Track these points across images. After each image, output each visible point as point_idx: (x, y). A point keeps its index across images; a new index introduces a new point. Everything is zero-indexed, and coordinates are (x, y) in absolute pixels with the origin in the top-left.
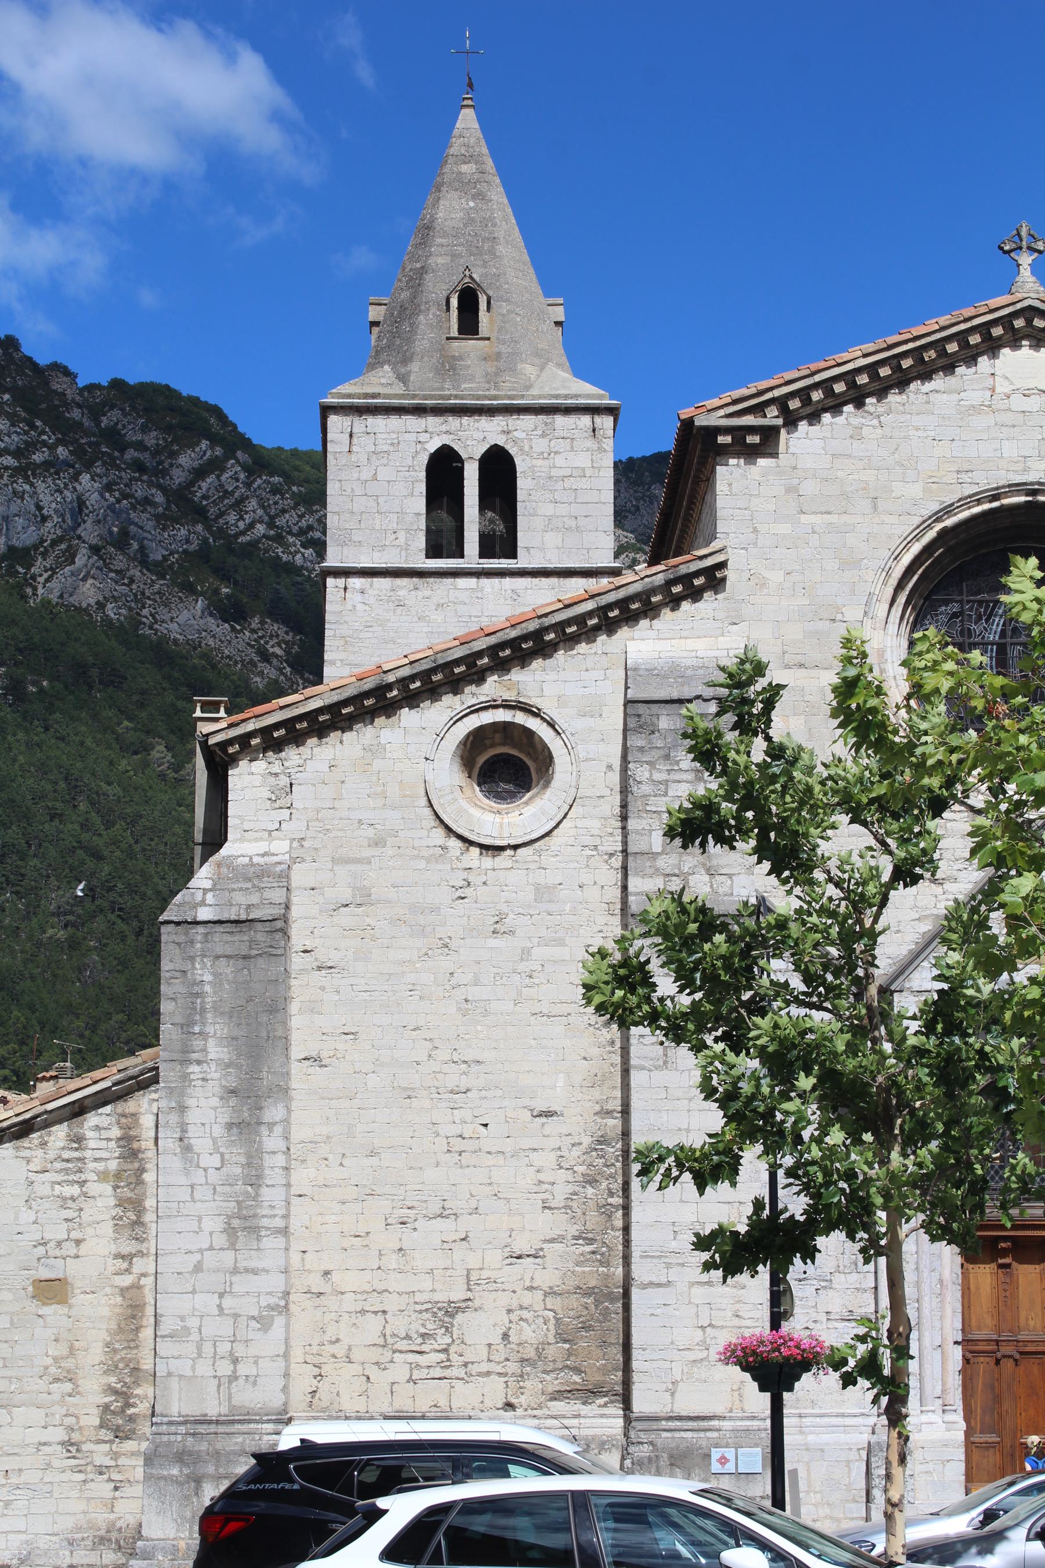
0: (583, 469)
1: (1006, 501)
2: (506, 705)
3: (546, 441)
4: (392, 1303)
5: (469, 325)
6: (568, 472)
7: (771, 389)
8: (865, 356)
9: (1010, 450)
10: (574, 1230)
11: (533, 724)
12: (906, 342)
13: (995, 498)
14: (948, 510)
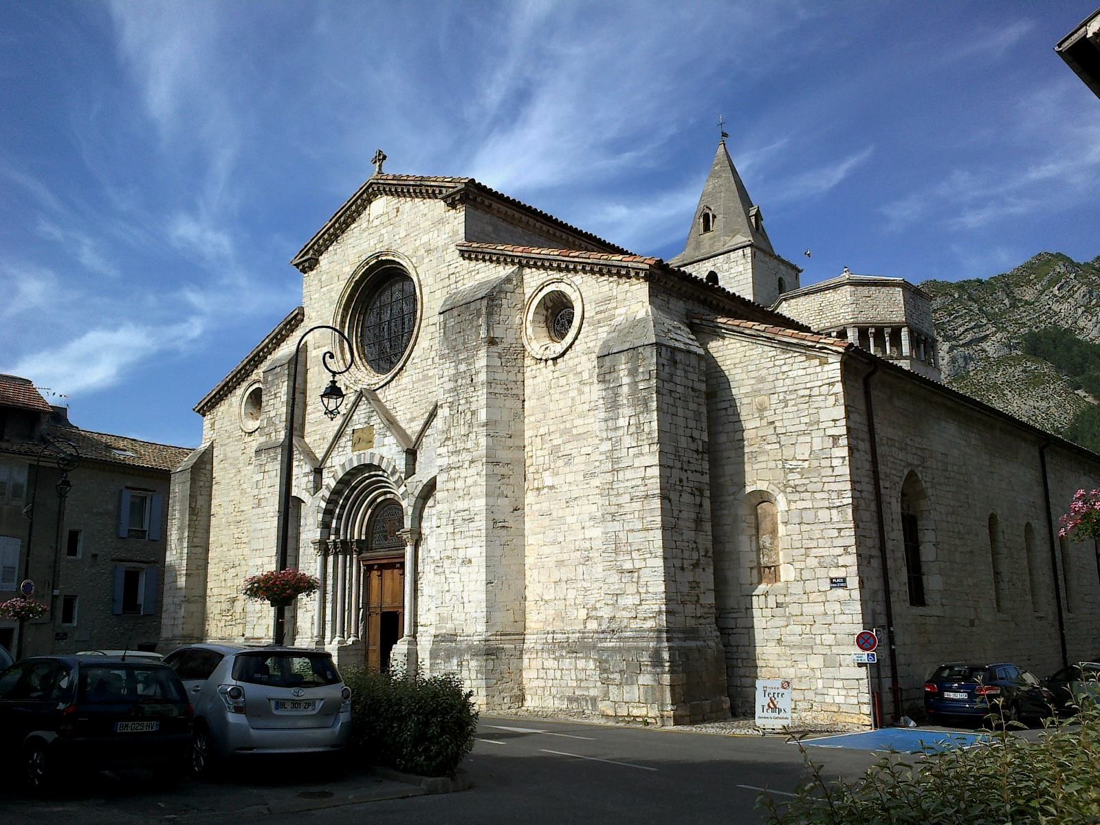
0: (741, 272)
1: (370, 264)
3: (727, 265)
4: (223, 598)
5: (707, 228)
6: (735, 275)
7: (308, 244)
8: (330, 222)
12: (339, 211)
13: (367, 263)
14: (355, 273)
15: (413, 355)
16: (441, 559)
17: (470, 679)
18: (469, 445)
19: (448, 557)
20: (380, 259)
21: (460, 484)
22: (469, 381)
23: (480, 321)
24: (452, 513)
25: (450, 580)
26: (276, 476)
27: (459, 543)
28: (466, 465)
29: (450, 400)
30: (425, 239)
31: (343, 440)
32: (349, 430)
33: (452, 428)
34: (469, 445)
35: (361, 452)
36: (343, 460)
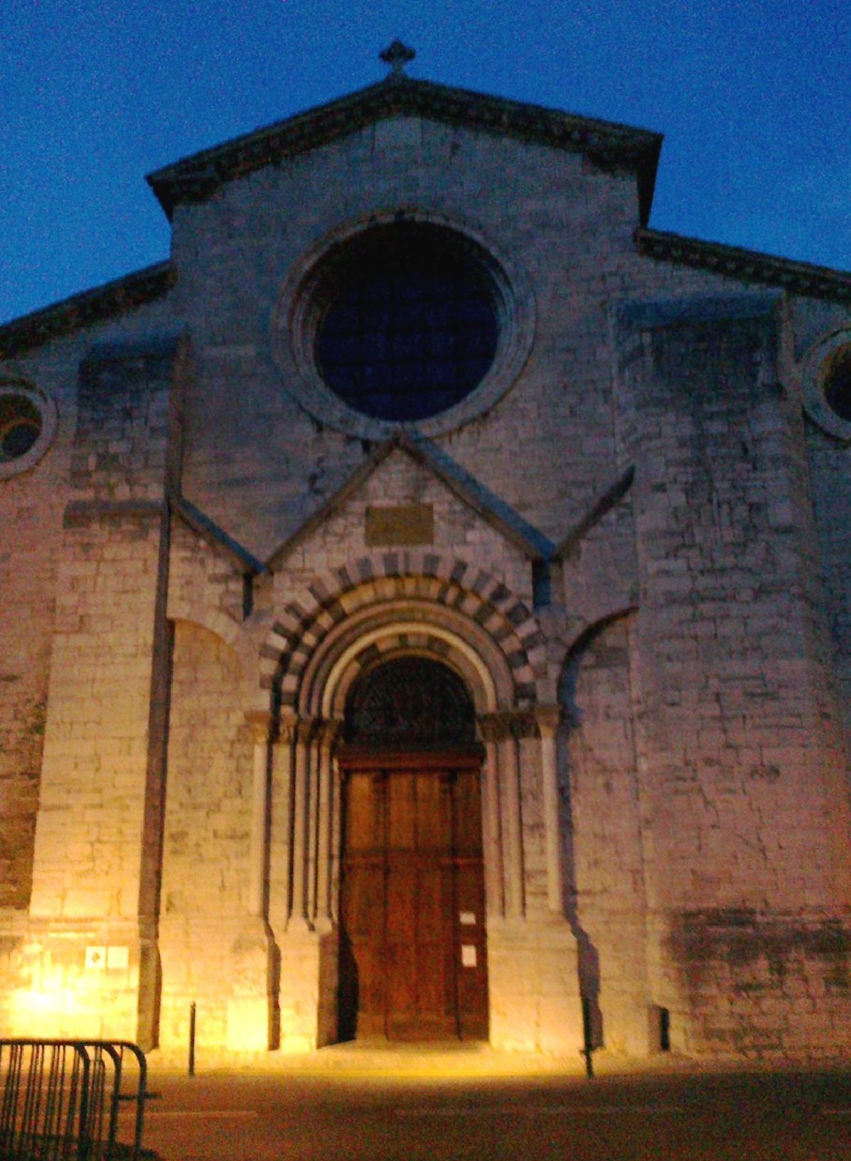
2: (13, 383)
9: (383, 185)
10: (20, 768)
11: (30, 395)
15: (515, 393)
16: (687, 763)
17: (809, 996)
18: (749, 561)
19: (709, 762)
20: (406, 216)
21: (728, 628)
22: (737, 451)
23: (758, 356)
24: (713, 682)
25: (720, 806)
26: (145, 571)
27: (739, 737)
28: (746, 595)
29: (682, 478)
30: (534, 205)
31: (338, 524)
32: (357, 506)
33: (697, 531)
34: (749, 561)
35: (394, 549)
36: (339, 560)
